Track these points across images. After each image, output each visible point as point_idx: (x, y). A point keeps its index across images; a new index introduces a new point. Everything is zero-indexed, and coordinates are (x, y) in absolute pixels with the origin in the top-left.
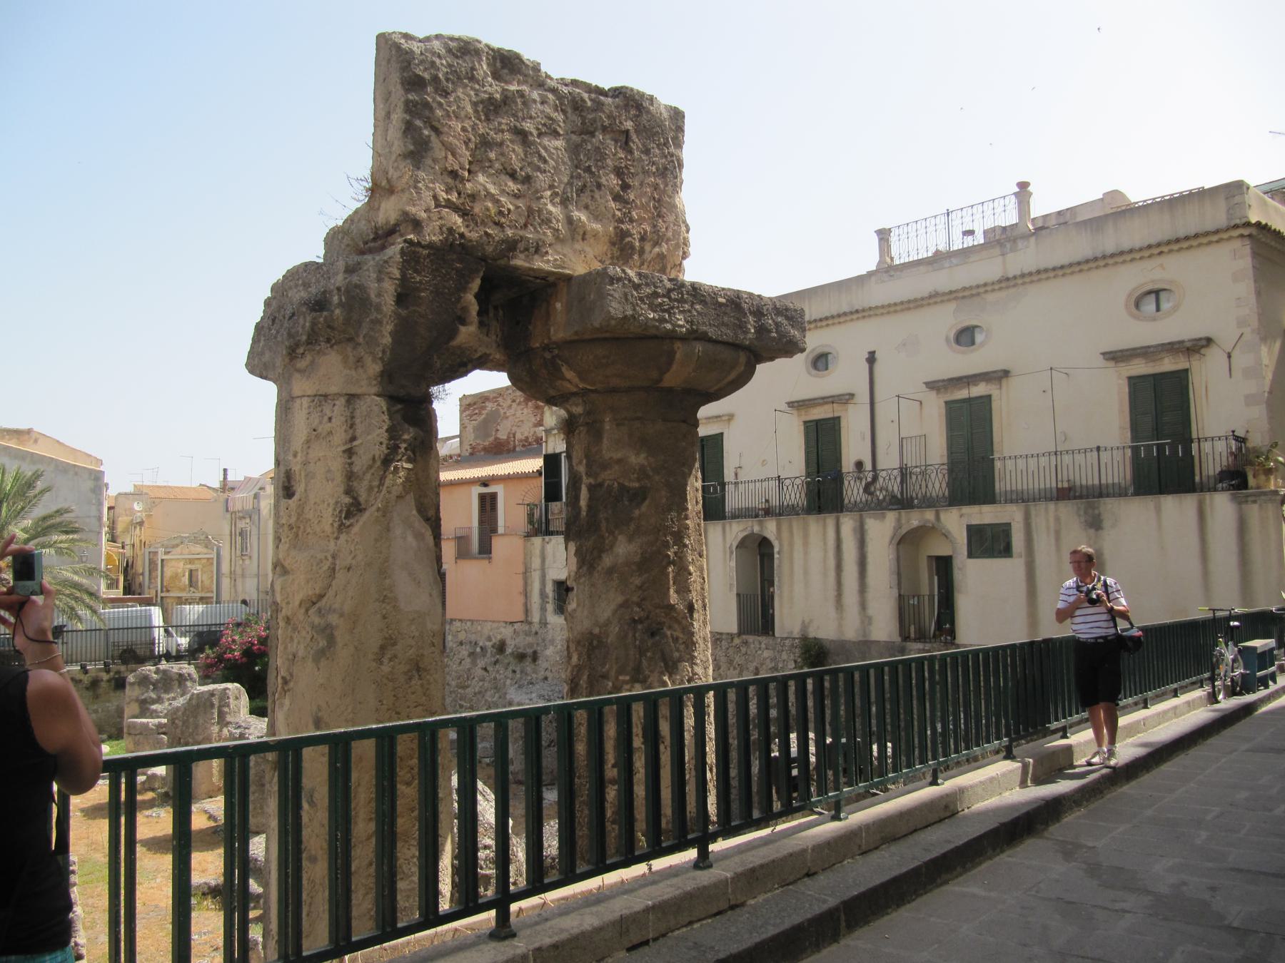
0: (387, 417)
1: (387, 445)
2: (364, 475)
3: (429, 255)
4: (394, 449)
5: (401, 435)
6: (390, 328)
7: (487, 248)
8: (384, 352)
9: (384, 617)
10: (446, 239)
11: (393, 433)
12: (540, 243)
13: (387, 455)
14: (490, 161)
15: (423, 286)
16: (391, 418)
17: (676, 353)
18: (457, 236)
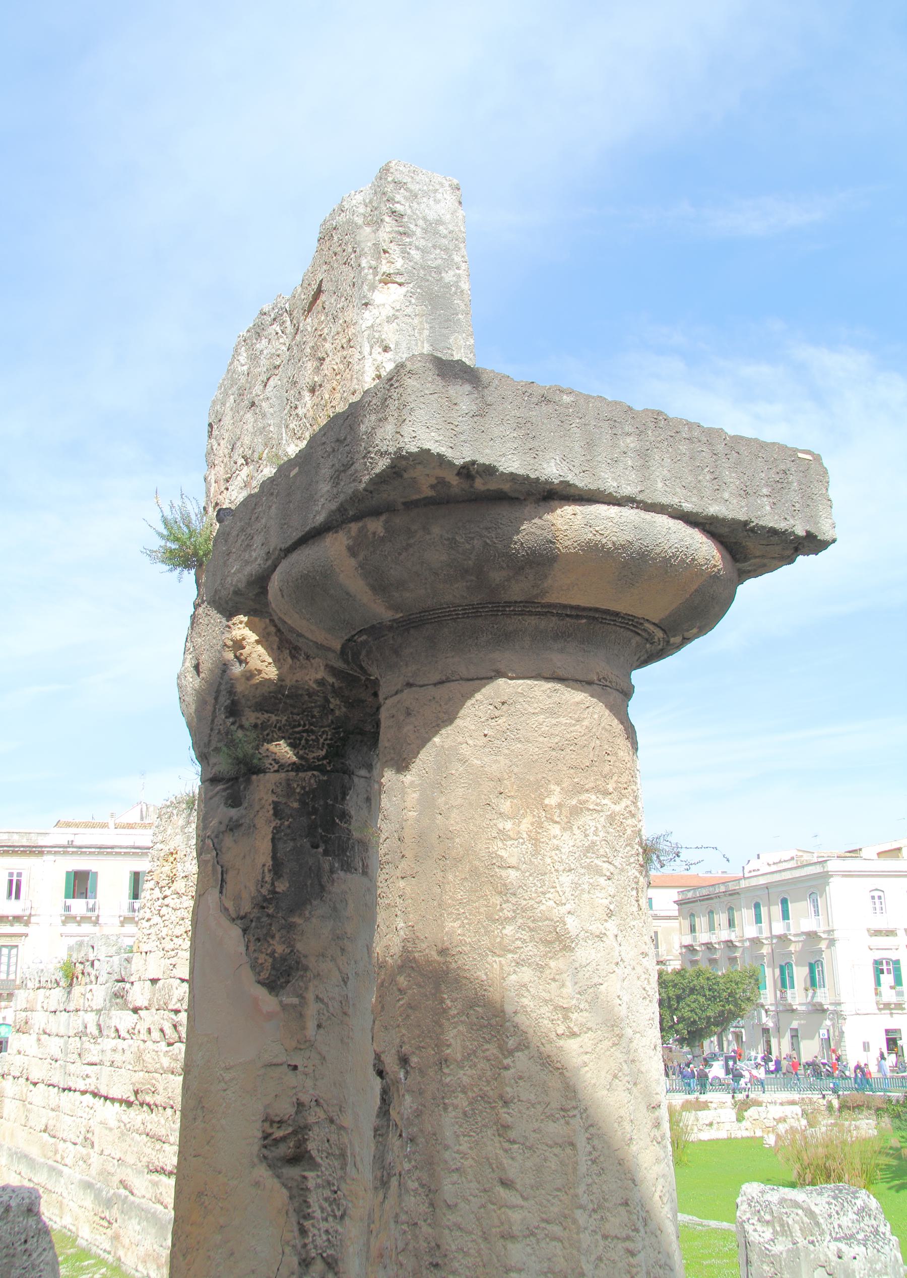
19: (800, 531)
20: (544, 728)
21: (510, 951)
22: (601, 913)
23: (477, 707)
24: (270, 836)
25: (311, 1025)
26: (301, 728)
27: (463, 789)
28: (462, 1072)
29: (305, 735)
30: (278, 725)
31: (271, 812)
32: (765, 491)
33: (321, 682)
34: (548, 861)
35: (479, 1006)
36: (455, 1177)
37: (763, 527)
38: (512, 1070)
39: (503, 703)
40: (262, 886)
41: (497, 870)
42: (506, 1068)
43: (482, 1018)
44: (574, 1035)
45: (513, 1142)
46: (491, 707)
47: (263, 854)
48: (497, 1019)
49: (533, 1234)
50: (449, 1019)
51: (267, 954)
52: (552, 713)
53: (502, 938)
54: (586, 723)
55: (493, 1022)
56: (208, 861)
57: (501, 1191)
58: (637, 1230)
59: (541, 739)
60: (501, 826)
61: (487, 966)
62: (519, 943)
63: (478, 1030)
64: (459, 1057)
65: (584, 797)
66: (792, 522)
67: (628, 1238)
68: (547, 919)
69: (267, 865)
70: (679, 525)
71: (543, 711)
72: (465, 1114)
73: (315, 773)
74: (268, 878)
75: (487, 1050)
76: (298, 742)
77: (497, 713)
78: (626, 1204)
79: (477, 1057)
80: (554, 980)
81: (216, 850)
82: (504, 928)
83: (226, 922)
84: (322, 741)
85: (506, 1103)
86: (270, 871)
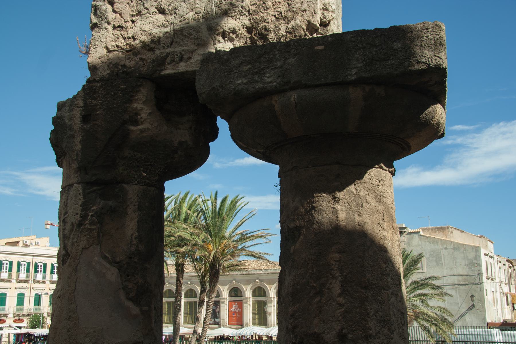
0: (82, 196)
1: (81, 214)
2: (70, 236)
3: (101, 86)
4: (84, 217)
5: (92, 207)
6: (79, 139)
7: (142, 69)
8: (77, 155)
9: (68, 331)
10: (112, 72)
11: (85, 206)
12: (183, 53)
13: (80, 221)
14: (147, 9)
15: (98, 107)
16: (84, 197)
17: (274, 106)
18: (120, 67)
21: (390, 288)
23: (372, 179)
24: (137, 220)
25: (153, 321)
26: (149, 163)
27: (369, 216)
28: (375, 341)
29: (150, 167)
30: (139, 159)
31: (137, 207)
33: (181, 143)
35: (380, 312)
38: (394, 339)
40: (131, 246)
41: (384, 253)
43: (381, 317)
46: (377, 181)
47: (132, 229)
48: (387, 317)
50: (370, 318)
51: (134, 283)
53: (388, 282)
55: (386, 319)
56: (91, 230)
60: (384, 234)
61: (382, 295)
63: (380, 322)
64: (374, 334)
68: (397, 275)
69: (135, 235)
73: (155, 188)
74: (135, 242)
75: (384, 331)
76: (146, 170)
77: (379, 184)
79: (380, 334)
80: (400, 301)
81: (99, 223)
82: (388, 278)
83: (108, 266)
84: (157, 172)
86: (136, 238)
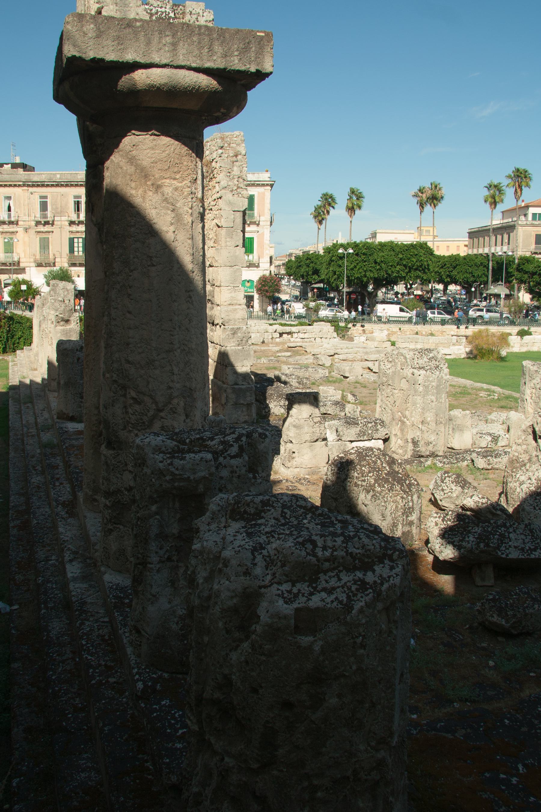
19: (253, 69)
20: (149, 155)
22: (168, 223)
32: (236, 53)
34: (147, 205)
36: (116, 310)
37: (234, 70)
39: (134, 146)
42: (130, 276)
44: (154, 266)
45: (132, 299)
49: (137, 328)
52: (153, 149)
54: (167, 152)
57: (128, 315)
58: (175, 329)
59: (148, 159)
62: (136, 234)
65: (163, 181)
66: (248, 66)
67: (171, 331)
70: (192, 72)
71: (149, 148)
72: (119, 291)
77: (132, 149)
78: (171, 320)
80: (147, 247)
85: (130, 287)
